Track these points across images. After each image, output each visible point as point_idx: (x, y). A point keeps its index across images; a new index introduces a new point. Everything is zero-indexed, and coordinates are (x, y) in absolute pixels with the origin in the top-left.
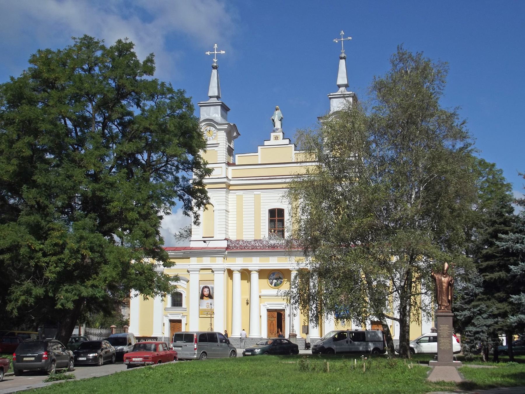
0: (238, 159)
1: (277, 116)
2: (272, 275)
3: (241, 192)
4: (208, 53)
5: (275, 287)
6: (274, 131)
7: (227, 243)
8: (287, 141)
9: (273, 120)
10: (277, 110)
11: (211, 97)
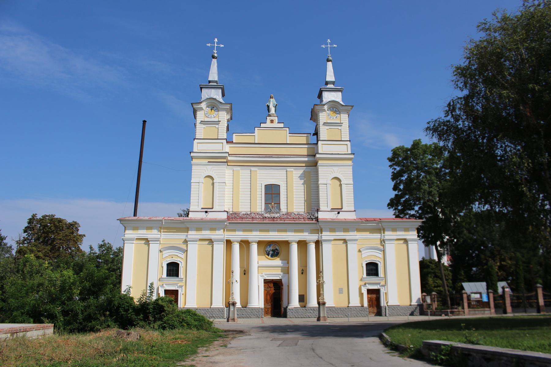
0: (235, 138)
1: (272, 103)
2: (268, 247)
3: (238, 168)
4: (209, 45)
5: (272, 258)
6: (270, 116)
7: (227, 215)
8: (282, 125)
9: (268, 106)
10: (271, 98)
11: (210, 82)
